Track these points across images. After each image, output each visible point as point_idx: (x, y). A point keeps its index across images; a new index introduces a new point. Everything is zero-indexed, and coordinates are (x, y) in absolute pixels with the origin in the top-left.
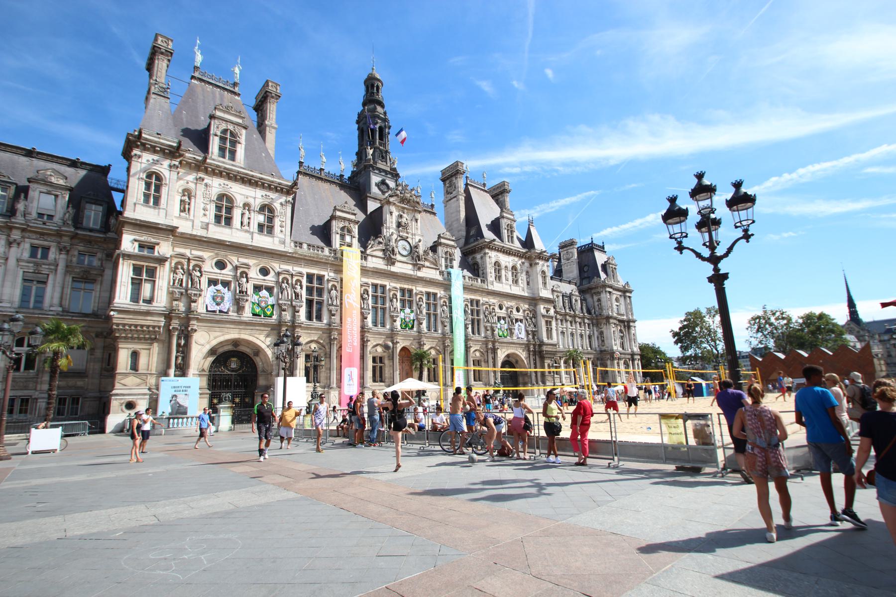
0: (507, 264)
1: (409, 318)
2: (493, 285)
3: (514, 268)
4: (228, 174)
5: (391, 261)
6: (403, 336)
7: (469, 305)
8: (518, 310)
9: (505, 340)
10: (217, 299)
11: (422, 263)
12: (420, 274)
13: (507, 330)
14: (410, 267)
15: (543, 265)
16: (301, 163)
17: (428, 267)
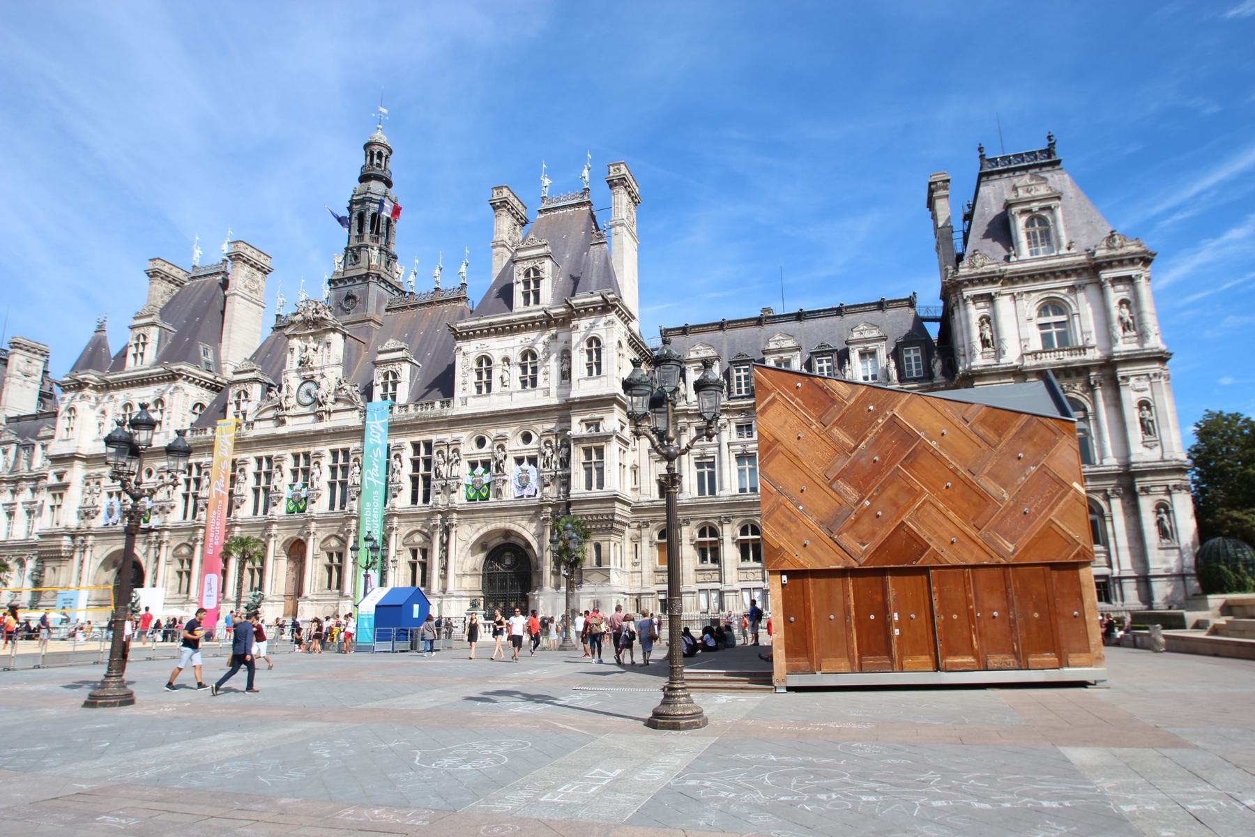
0: (510, 354)
1: (299, 495)
2: (465, 402)
3: (529, 354)
4: (127, 382)
5: (280, 421)
6: (288, 523)
7: (408, 454)
8: (527, 438)
9: (482, 505)
10: (110, 513)
11: (329, 407)
12: (320, 426)
13: (488, 485)
14: (312, 418)
15: (592, 326)
16: (278, 316)
17: (335, 411)
